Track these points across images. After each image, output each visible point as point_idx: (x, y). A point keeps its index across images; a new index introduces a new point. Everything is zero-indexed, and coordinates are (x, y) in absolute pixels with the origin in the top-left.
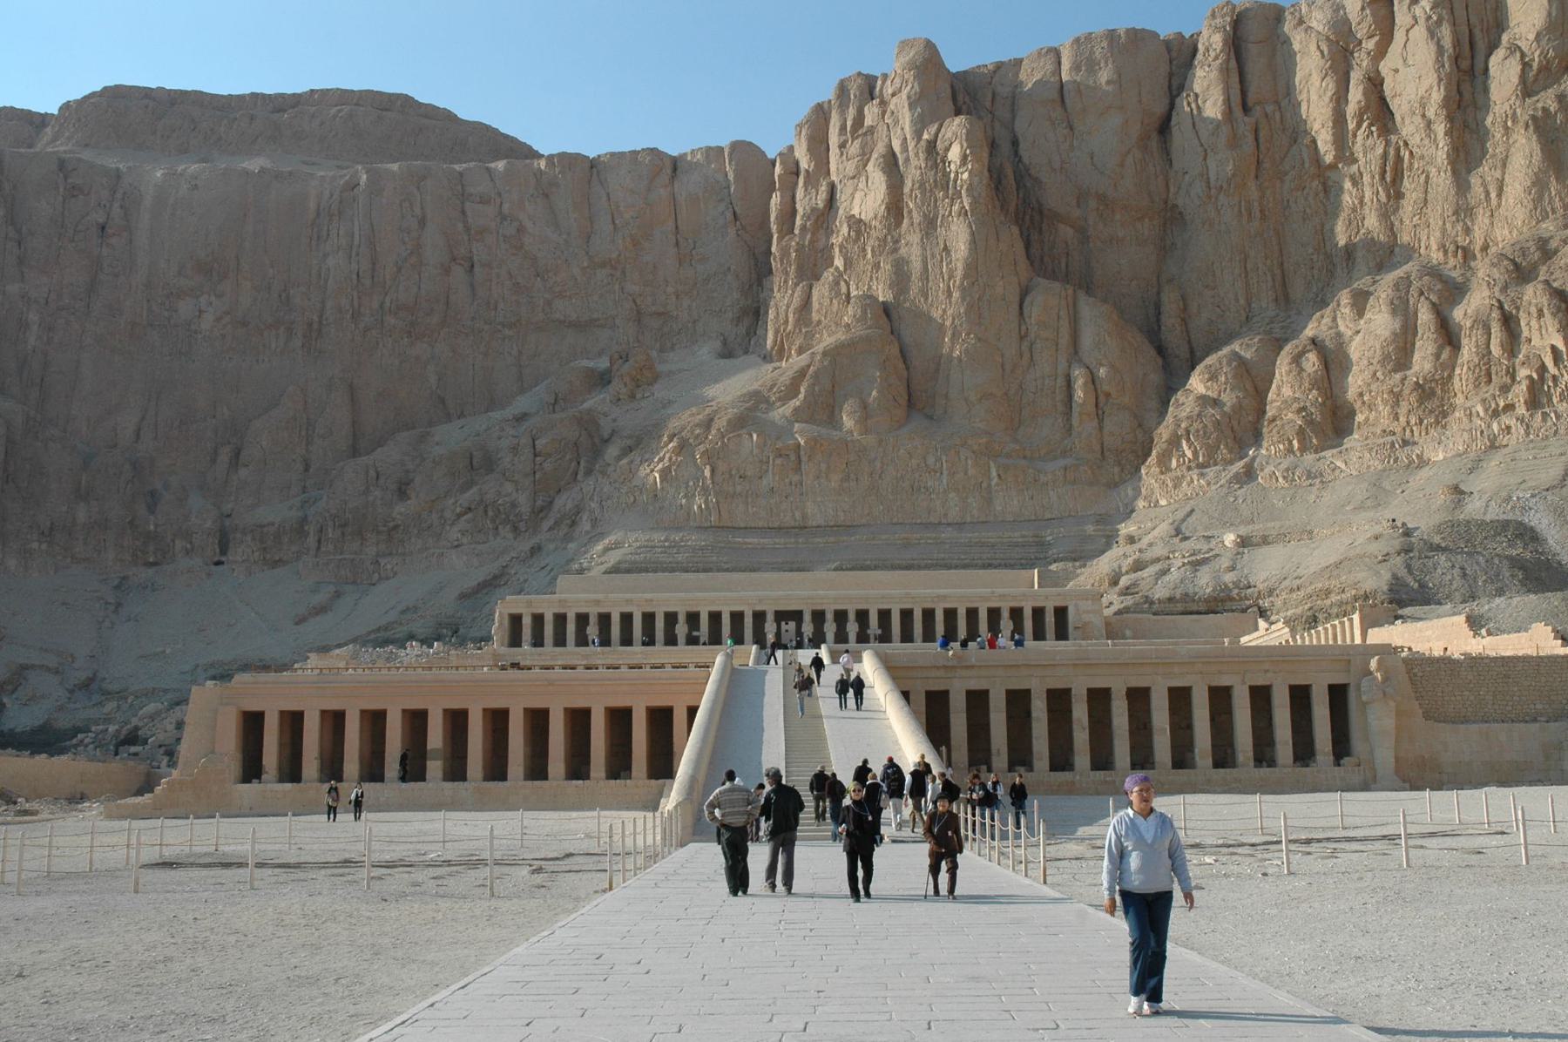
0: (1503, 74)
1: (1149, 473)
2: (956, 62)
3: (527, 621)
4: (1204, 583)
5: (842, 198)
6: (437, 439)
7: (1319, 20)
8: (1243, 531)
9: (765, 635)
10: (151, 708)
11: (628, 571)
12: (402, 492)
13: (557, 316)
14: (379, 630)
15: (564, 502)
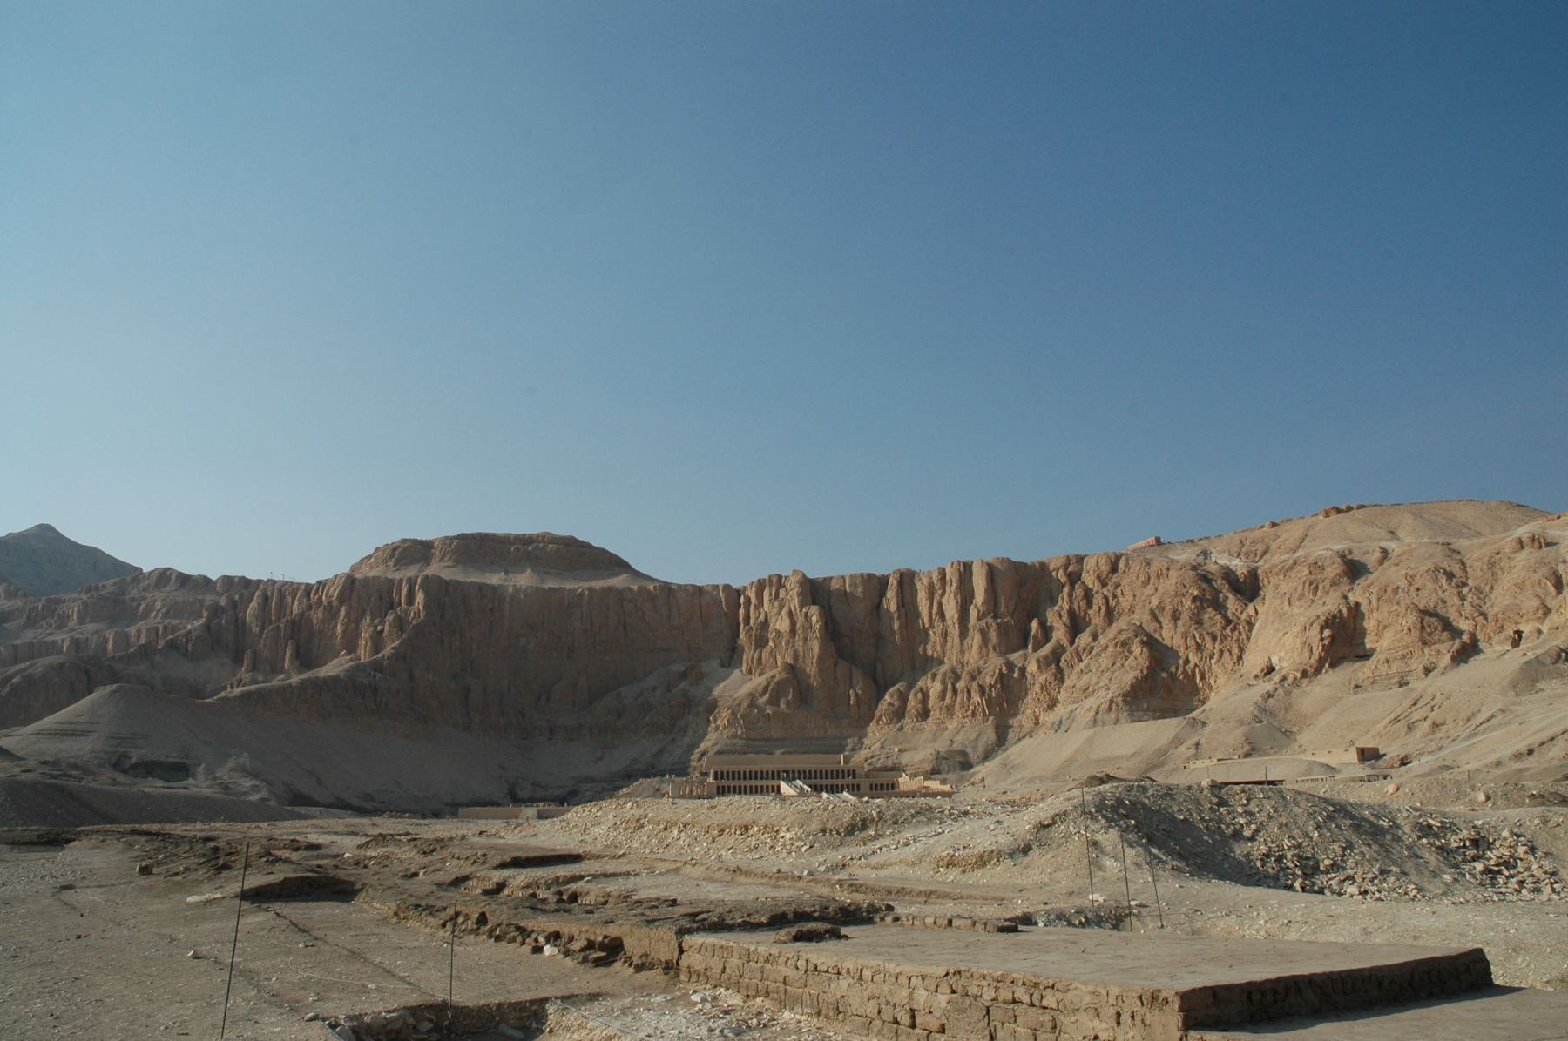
0: (973, 613)
1: (872, 727)
2: (810, 576)
4: (890, 763)
5: (772, 621)
7: (925, 581)
12: (619, 716)
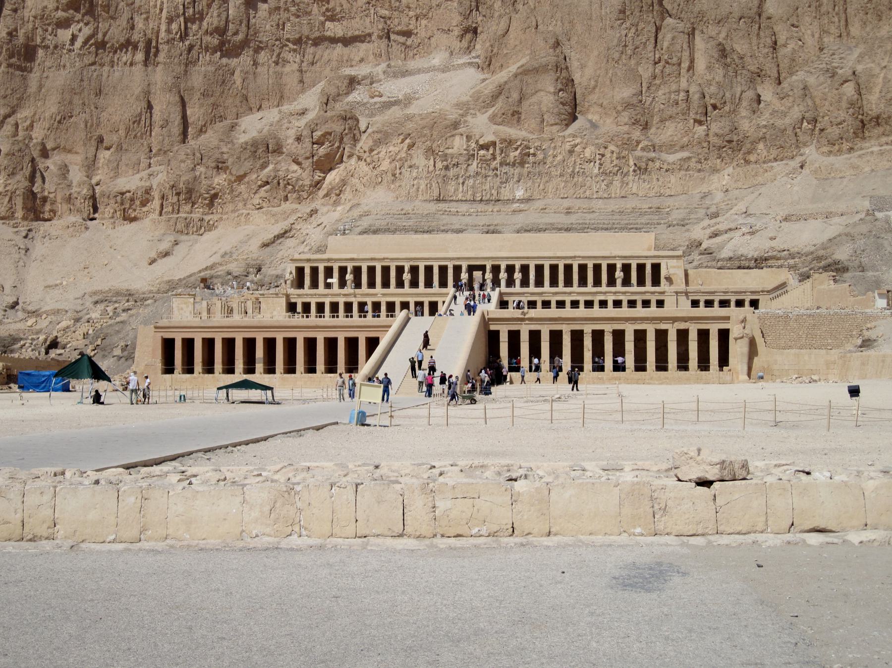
3: (307, 271)
6: (243, 128)
8: (787, 212)
10: (64, 324)
11: (375, 232)
13: (328, 34)
14: (206, 269)
15: (333, 177)
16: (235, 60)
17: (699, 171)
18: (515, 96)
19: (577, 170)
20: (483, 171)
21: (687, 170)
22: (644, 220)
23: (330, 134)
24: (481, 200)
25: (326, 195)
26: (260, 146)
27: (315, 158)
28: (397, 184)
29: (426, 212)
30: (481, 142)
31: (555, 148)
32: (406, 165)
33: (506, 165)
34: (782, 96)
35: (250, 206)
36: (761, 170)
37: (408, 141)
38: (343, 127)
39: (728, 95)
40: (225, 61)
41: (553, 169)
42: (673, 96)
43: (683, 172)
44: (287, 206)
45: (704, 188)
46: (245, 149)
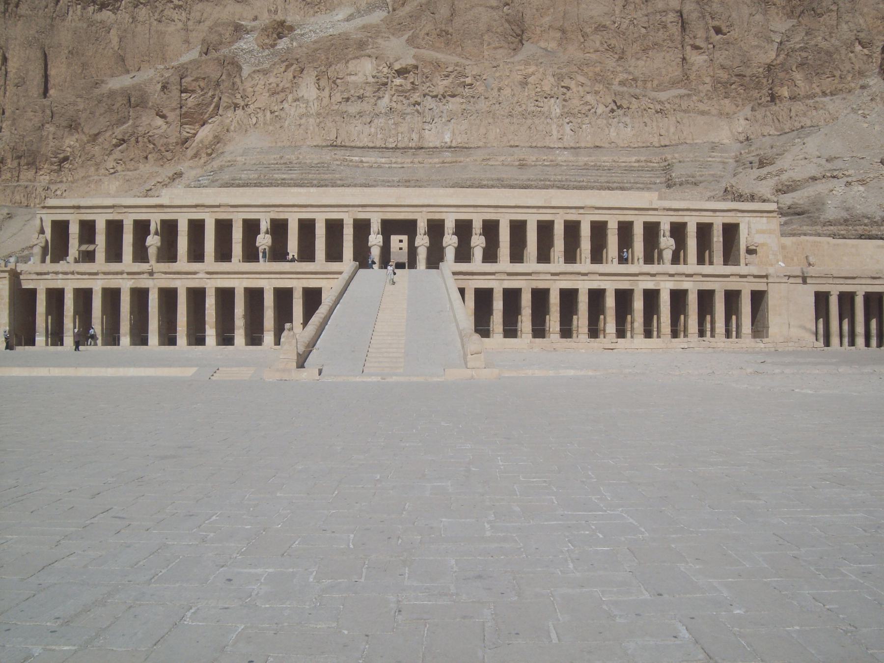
9: (368, 249)
11: (239, 186)
15: (205, 133)
16: (113, 16)
17: (703, 113)
18: (444, 11)
19: (534, 109)
20: (399, 107)
21: (685, 111)
22: (632, 177)
23: (204, 79)
24: (396, 148)
25: (196, 155)
26: (119, 99)
27: (184, 110)
28: (278, 126)
29: (316, 162)
30: (397, 66)
31: (500, 77)
32: (290, 98)
33: (433, 97)
34: (819, 11)
35: (103, 171)
36: (804, 108)
37: (295, 66)
38: (219, 74)
39: (734, 15)
40: (99, 17)
41: (497, 105)
42: (658, 17)
43: (679, 115)
44: (145, 168)
45: (713, 137)
46: (100, 102)
